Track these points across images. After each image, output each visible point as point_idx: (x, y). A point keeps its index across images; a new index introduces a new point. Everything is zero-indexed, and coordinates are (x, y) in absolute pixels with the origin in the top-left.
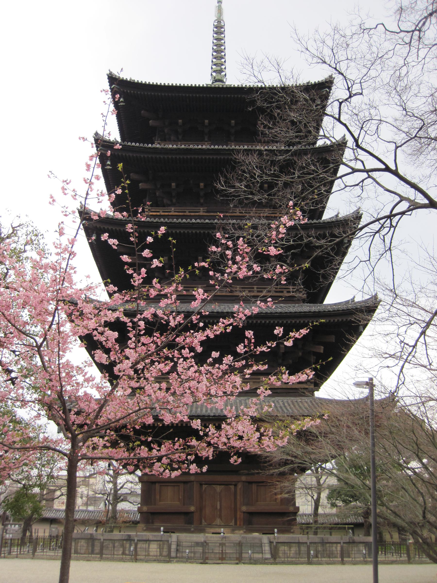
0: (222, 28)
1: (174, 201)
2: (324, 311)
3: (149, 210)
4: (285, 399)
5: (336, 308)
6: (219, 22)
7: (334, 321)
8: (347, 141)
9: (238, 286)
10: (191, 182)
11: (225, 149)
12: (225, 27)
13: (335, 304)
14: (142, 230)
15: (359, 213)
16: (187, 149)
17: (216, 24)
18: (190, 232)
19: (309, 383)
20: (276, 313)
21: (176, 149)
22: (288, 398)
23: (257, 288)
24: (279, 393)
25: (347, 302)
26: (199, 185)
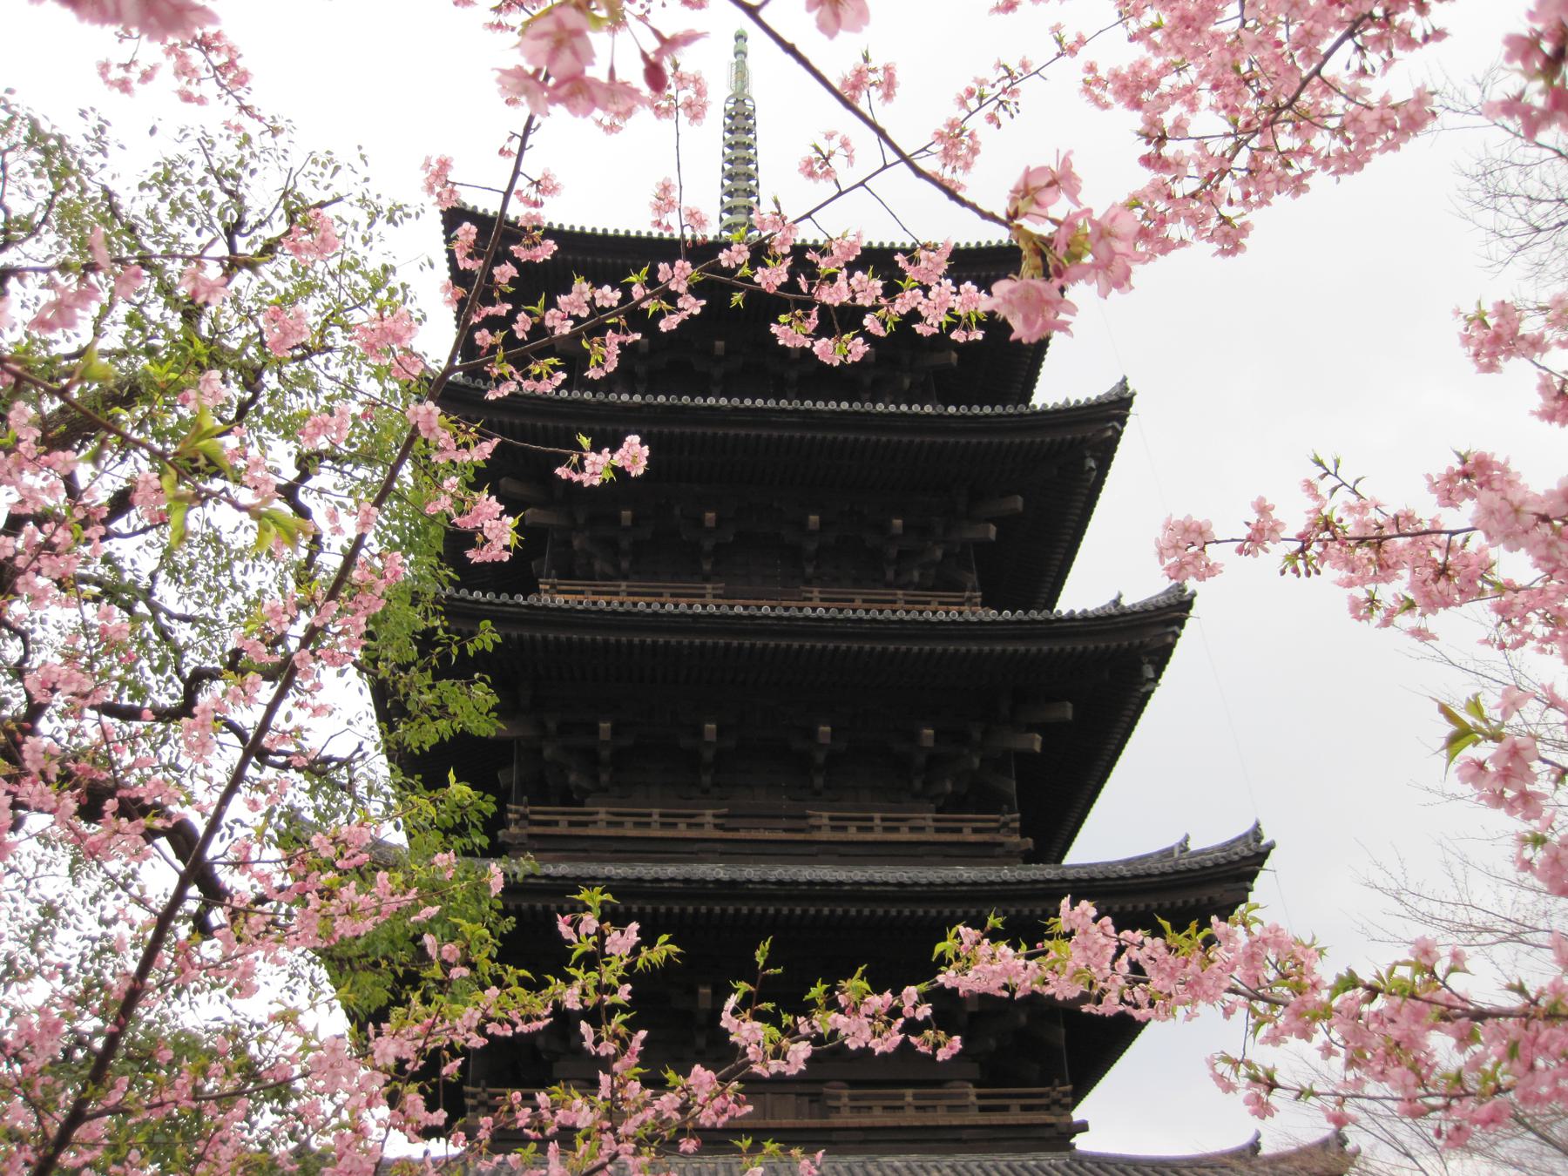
0: (748, 117)
1: (625, 565)
2: (1107, 879)
3: (553, 586)
4: (988, 1160)
5: (1141, 870)
6: (740, 101)
7: (1135, 907)
8: (1134, 394)
9: (826, 814)
10: (677, 511)
11: (783, 411)
12: (758, 115)
13: (1128, 862)
14: (538, 635)
15: (1184, 590)
16: (673, 406)
17: (729, 106)
18: (686, 642)
19: (1056, 1109)
20: (962, 883)
21: (639, 407)
22: (995, 1157)
23: (883, 819)
24: (966, 1142)
25: (1168, 853)
26: (699, 522)
